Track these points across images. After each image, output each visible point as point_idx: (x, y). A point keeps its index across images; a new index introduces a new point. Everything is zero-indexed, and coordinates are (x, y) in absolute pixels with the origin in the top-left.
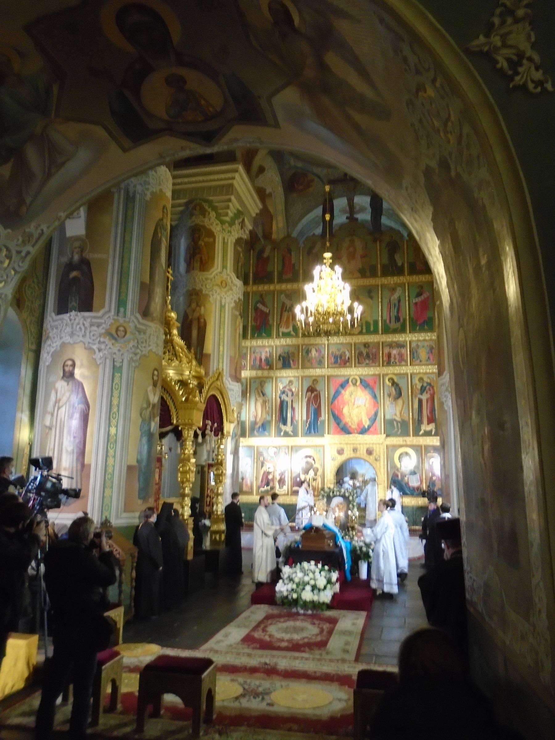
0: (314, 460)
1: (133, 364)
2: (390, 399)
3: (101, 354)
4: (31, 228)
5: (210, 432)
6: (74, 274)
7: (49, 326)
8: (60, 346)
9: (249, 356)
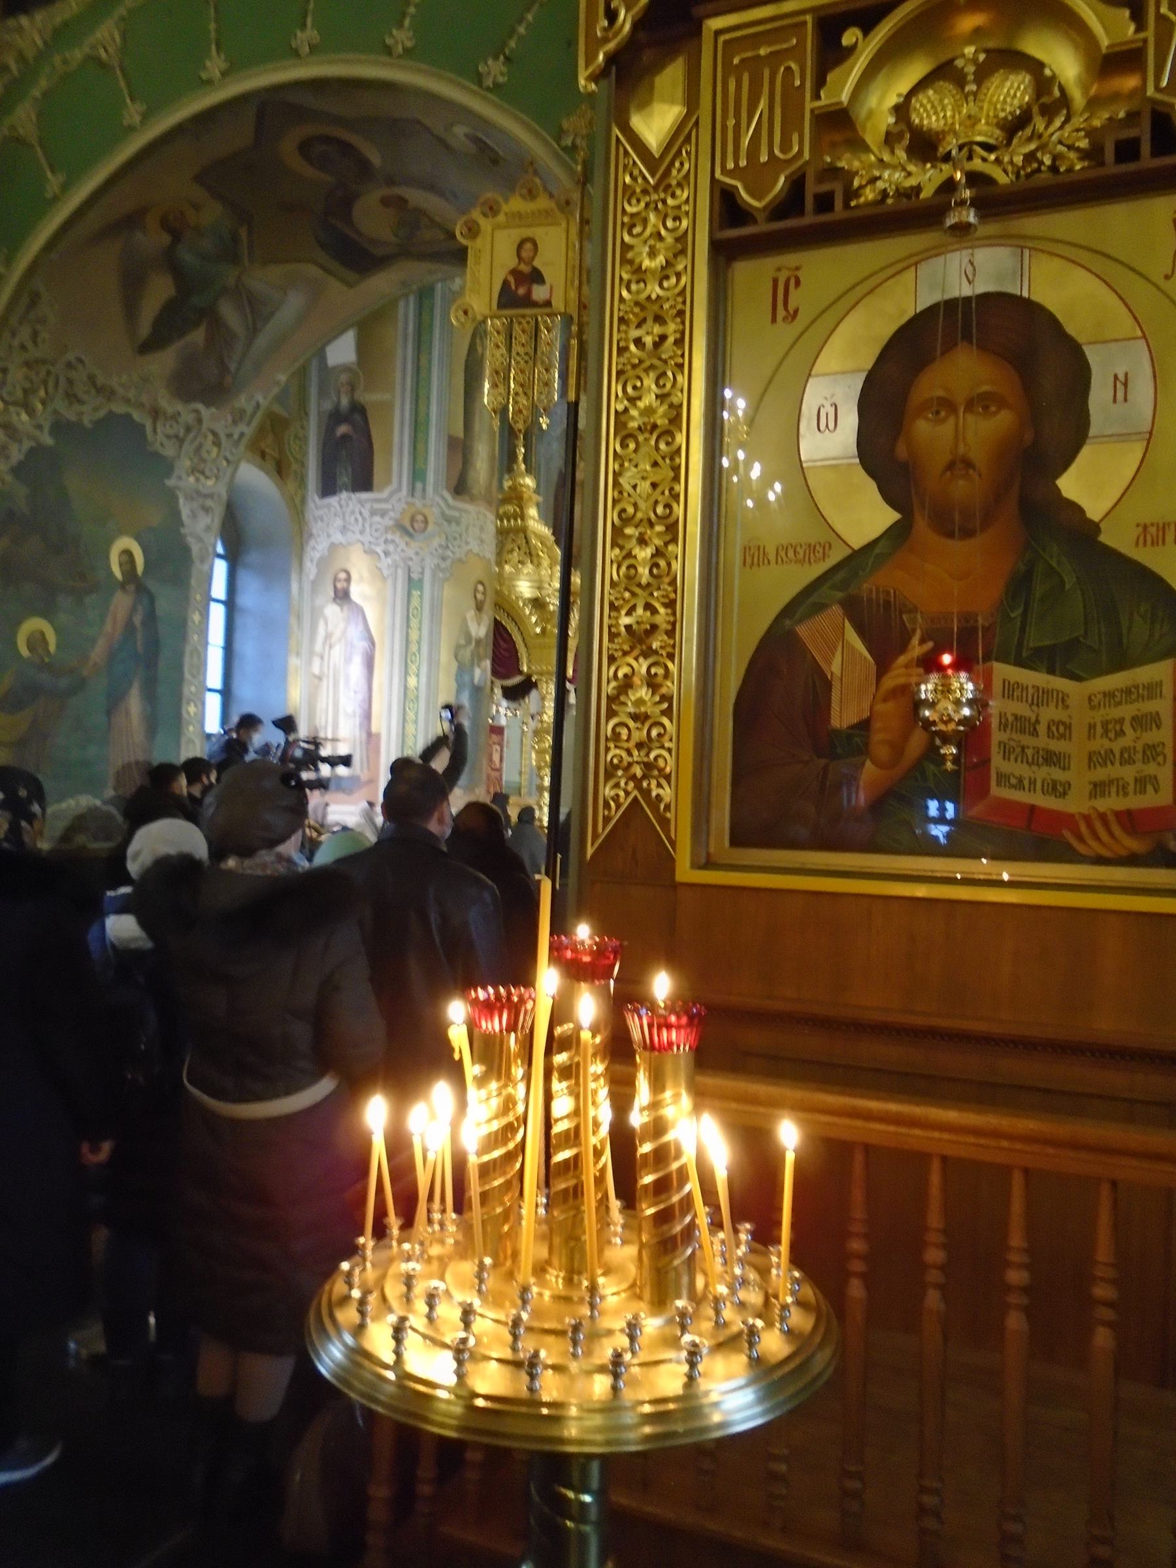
1: (441, 575)
3: (389, 560)
4: (242, 401)
6: (343, 429)
7: (311, 517)
8: (329, 550)
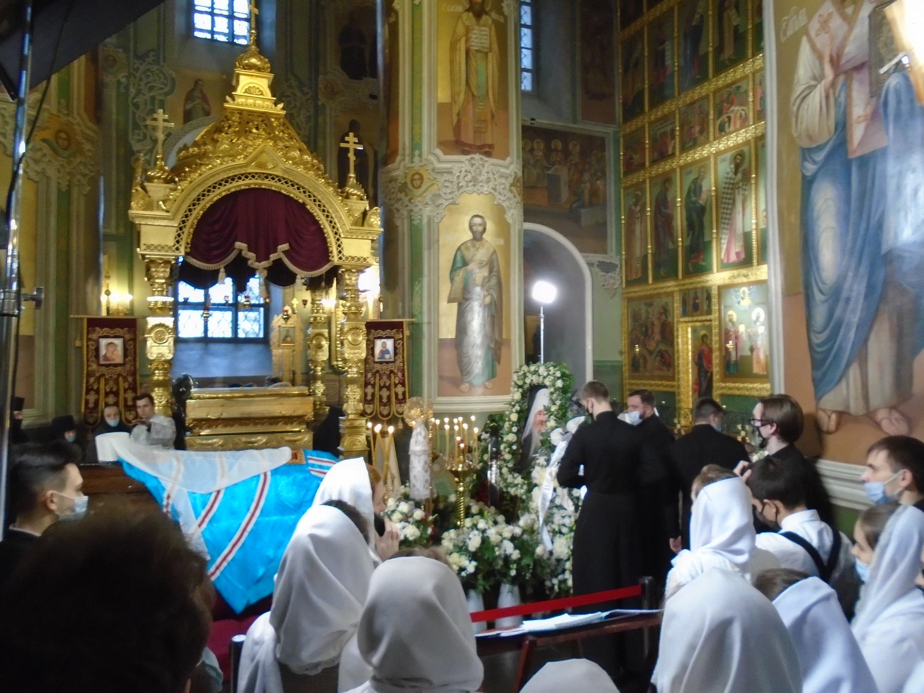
5: (257, 264)
9: (751, 94)
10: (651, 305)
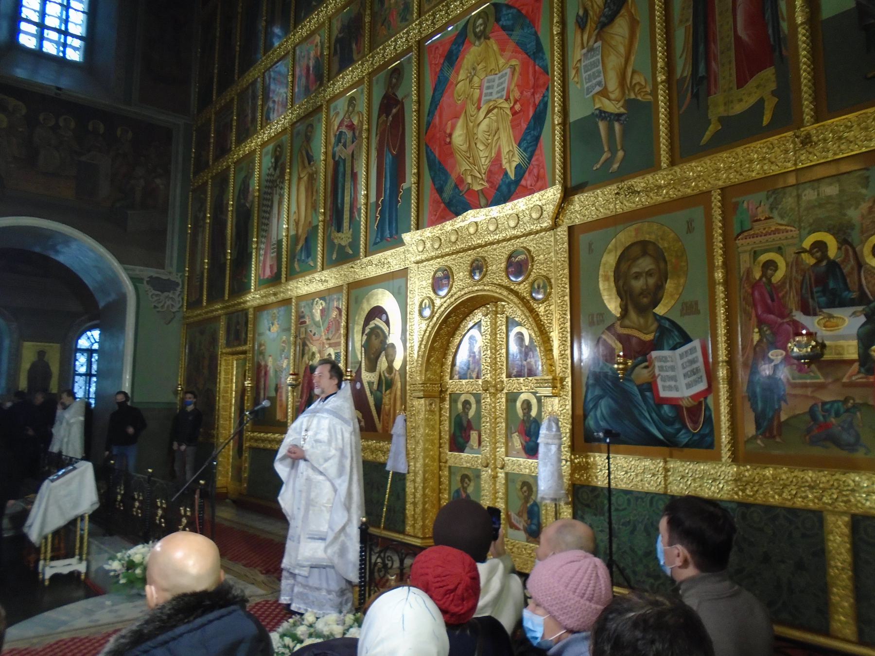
0: (387, 322)
2: (585, 37)
10: (202, 333)
